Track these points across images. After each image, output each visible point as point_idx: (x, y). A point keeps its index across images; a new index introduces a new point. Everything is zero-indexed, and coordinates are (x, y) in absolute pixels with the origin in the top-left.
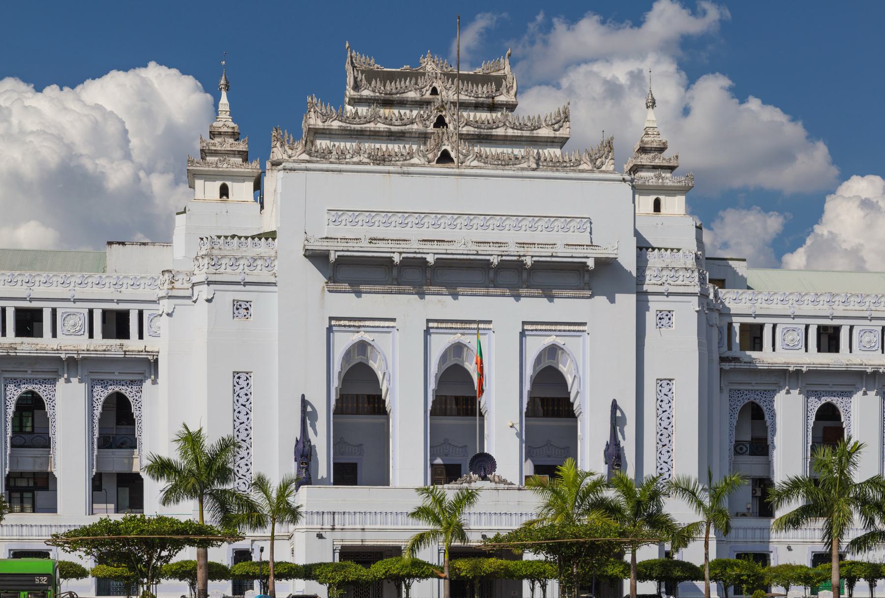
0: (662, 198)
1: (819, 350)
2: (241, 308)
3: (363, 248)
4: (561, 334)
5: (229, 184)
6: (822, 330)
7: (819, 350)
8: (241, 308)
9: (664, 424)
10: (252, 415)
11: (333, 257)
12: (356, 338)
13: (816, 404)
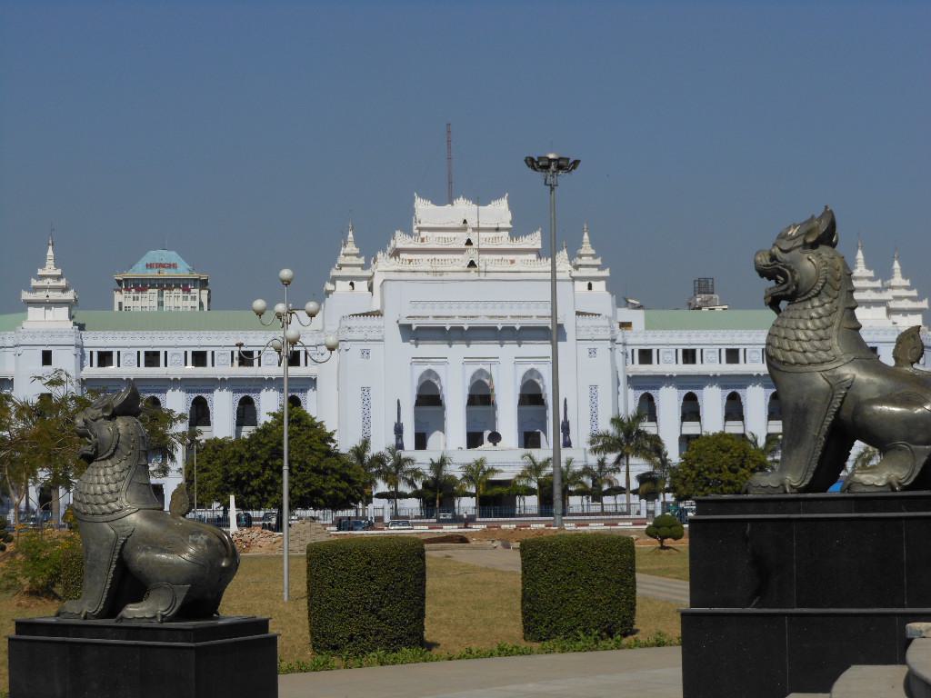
0: (593, 283)
1: (684, 363)
2: (365, 353)
3: (431, 322)
4: (536, 363)
5: (354, 282)
6: (685, 352)
7: (684, 363)
8: (365, 353)
9: (594, 409)
10: (371, 410)
11: (414, 327)
12: (426, 368)
13: (685, 392)
